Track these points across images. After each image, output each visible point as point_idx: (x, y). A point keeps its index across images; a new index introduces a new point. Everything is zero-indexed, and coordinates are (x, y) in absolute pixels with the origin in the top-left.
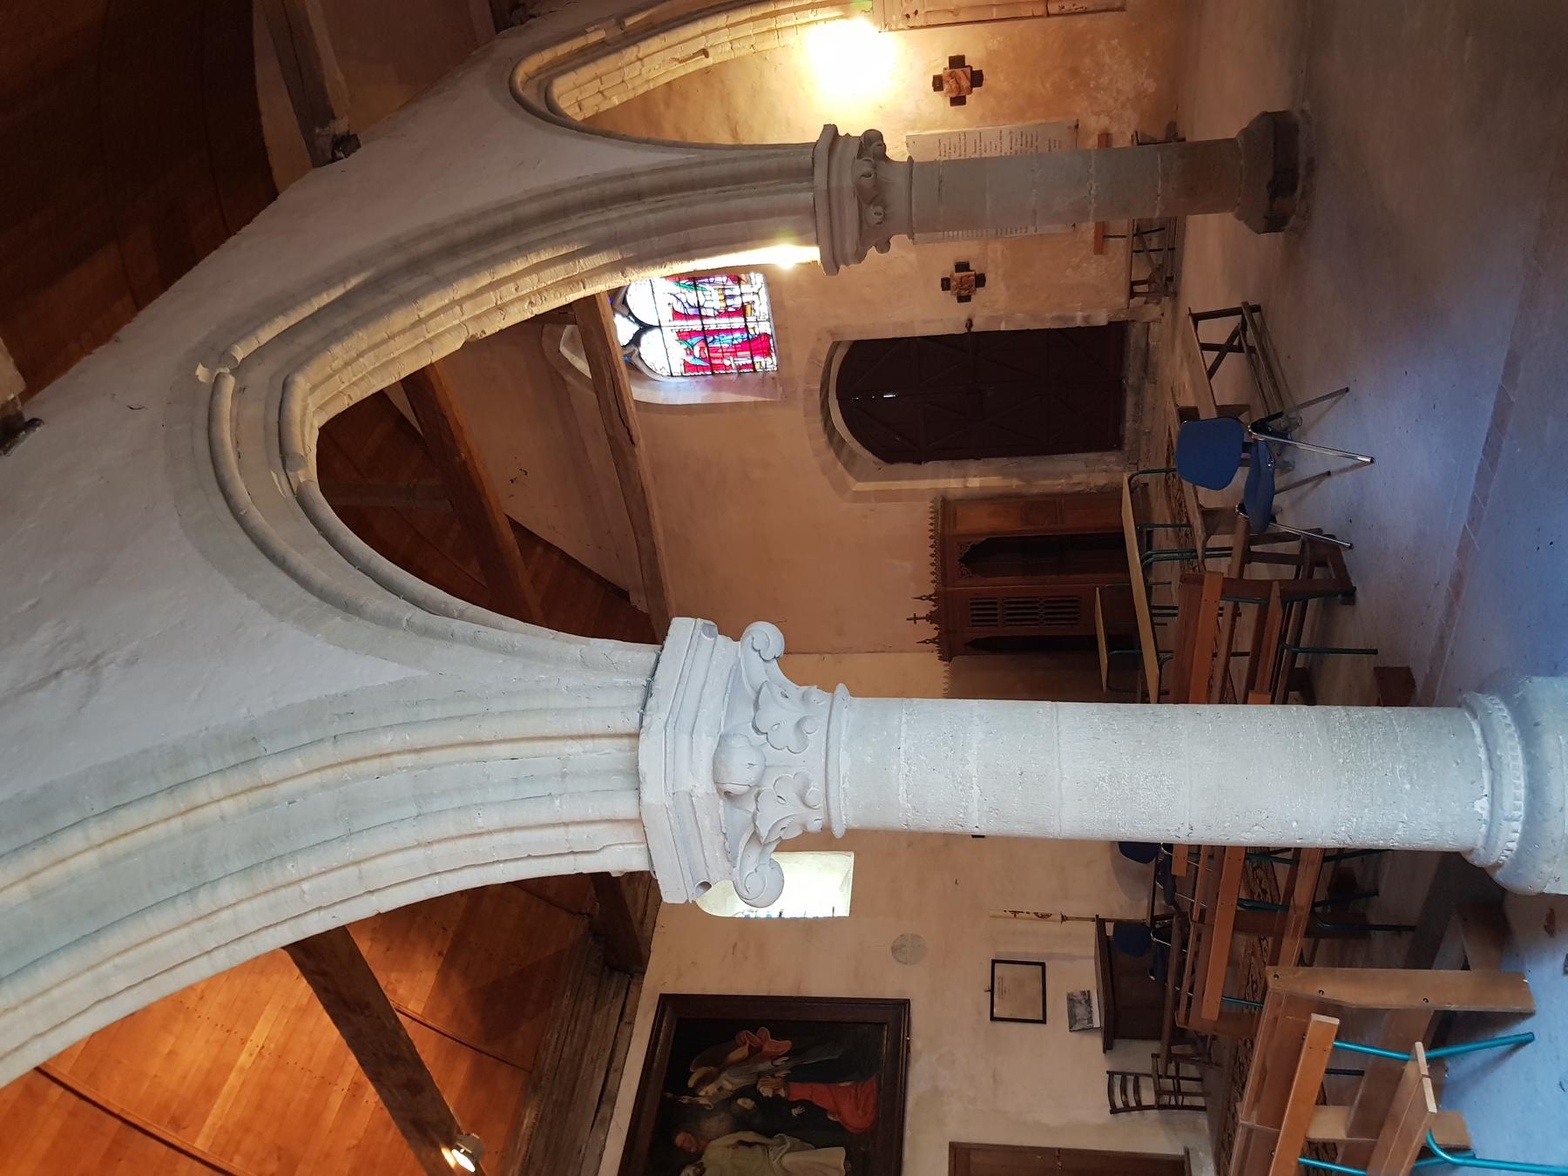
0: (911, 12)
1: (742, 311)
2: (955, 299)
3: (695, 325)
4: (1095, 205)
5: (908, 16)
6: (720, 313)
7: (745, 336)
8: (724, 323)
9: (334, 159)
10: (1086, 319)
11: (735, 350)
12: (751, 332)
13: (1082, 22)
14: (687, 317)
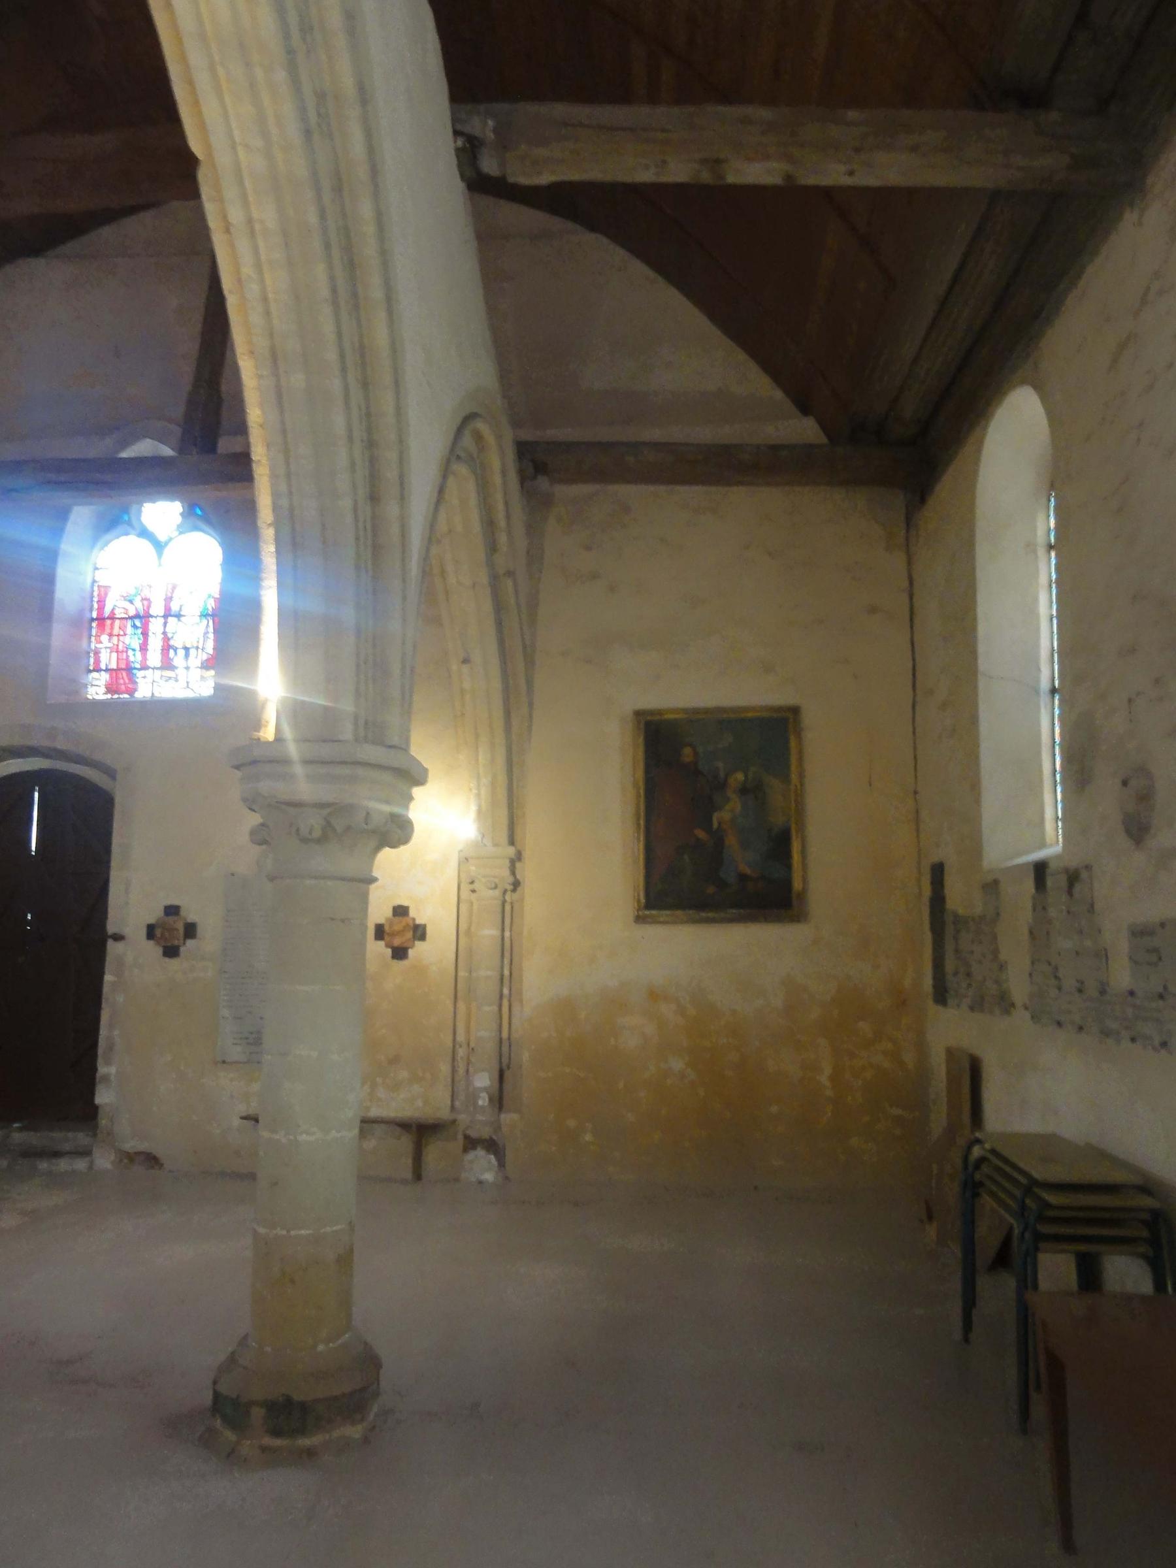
0: (476, 886)
1: (167, 665)
2: (152, 921)
4: (284, 1140)
5: (472, 882)
6: (169, 639)
7: (138, 666)
8: (155, 643)
9: (457, 133)
10: (106, 1078)
12: (142, 673)
13: (445, 1068)
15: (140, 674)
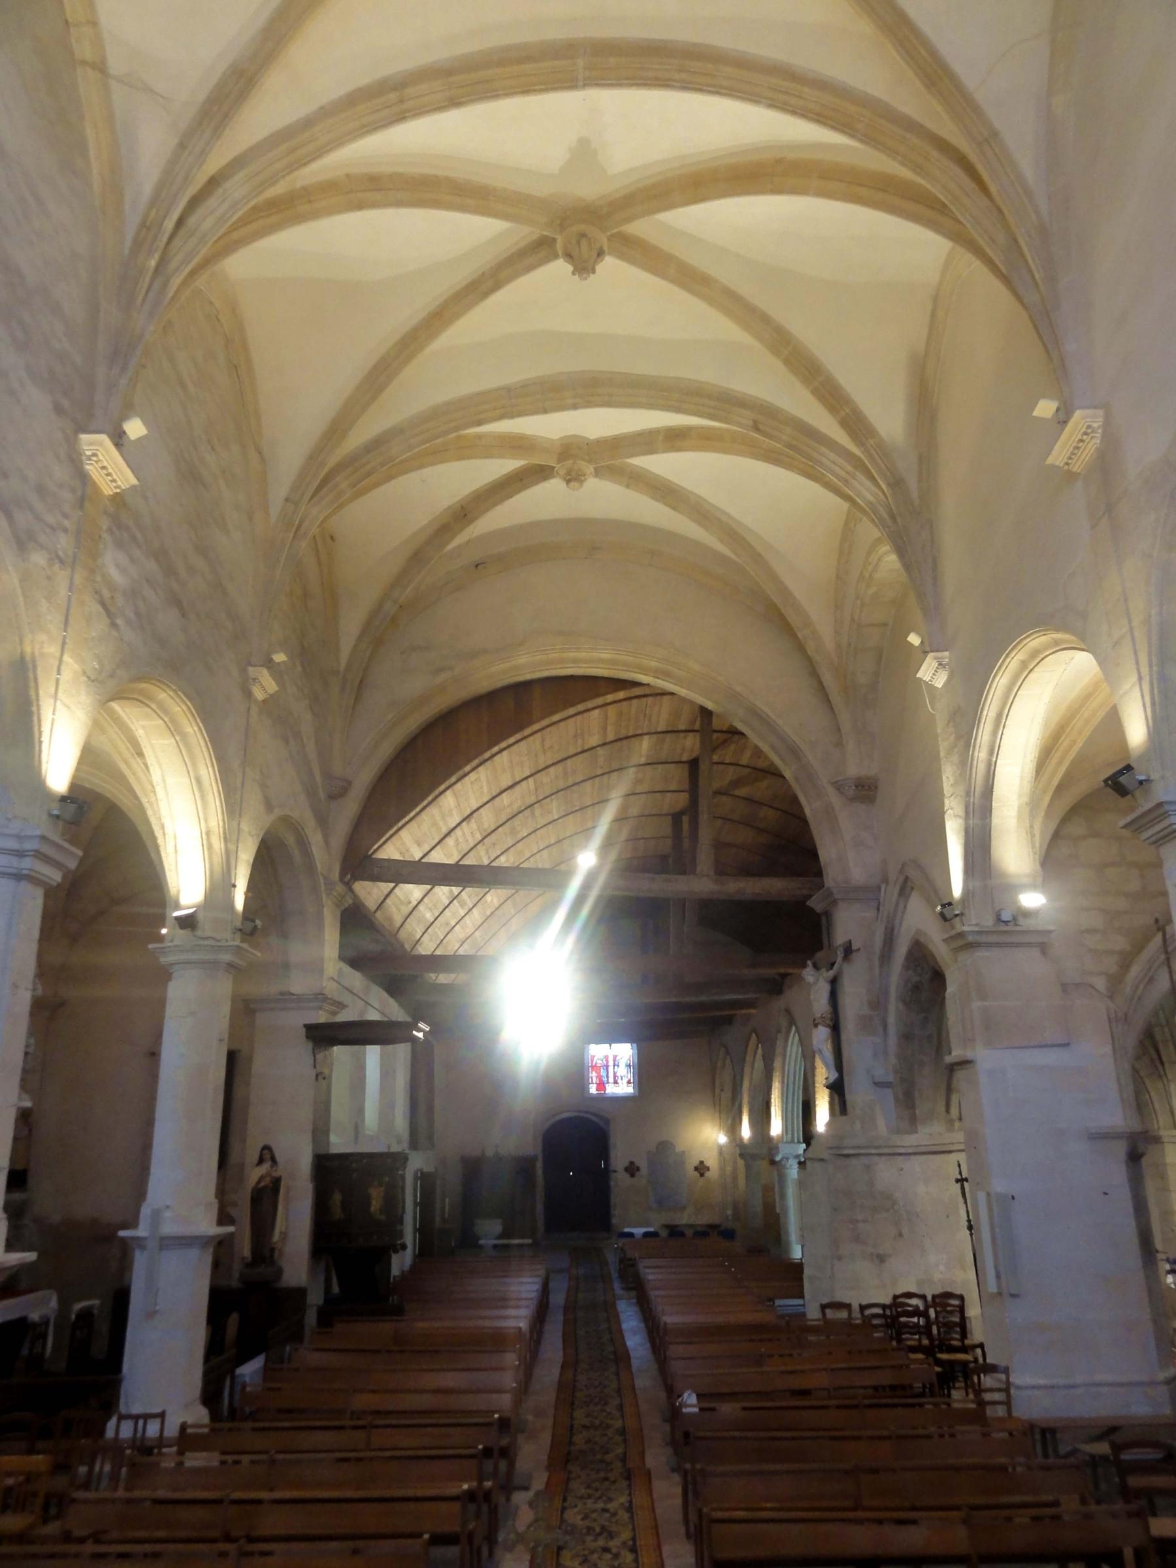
1: (616, 1082)
3: (611, 1063)
11: (599, 1077)
14: (614, 1061)
15: (607, 1085)
